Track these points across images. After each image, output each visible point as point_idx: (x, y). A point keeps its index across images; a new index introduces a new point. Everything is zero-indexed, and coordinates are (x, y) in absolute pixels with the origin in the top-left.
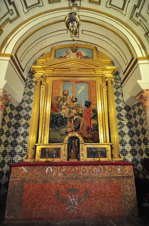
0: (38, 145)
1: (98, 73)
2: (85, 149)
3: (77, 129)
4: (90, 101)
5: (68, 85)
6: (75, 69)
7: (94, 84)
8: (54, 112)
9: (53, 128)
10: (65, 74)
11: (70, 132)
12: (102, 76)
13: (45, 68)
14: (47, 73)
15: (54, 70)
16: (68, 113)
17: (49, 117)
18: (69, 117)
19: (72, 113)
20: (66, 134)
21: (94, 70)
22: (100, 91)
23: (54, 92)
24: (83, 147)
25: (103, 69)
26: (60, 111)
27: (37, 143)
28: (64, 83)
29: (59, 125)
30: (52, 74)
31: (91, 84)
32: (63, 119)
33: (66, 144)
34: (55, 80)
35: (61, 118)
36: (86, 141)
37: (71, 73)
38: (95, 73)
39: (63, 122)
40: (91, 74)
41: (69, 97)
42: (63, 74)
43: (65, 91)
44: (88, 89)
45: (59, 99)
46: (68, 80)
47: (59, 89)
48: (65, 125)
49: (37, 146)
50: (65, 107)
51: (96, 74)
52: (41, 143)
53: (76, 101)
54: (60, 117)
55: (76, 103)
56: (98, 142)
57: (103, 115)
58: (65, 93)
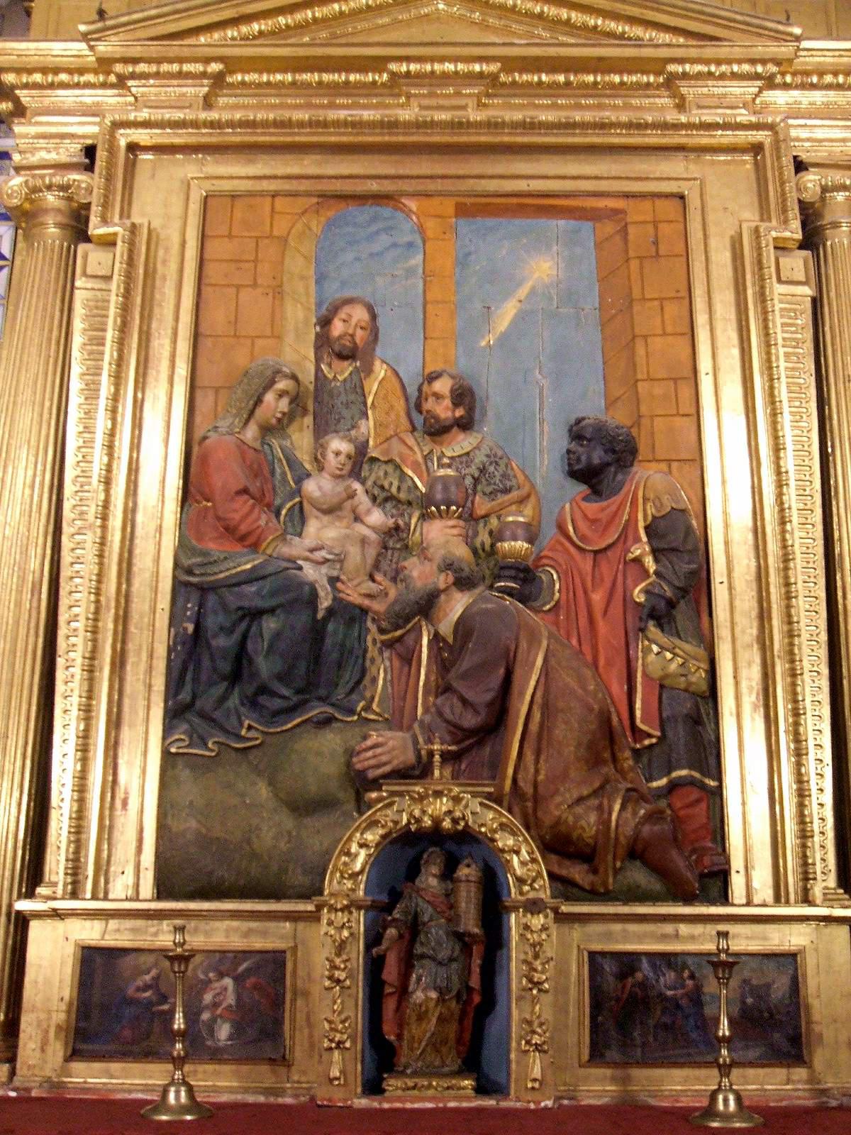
0: (39, 915)
1: (708, 117)
2: (562, 972)
3: (480, 743)
4: (619, 418)
5: (371, 237)
6: (449, 67)
7: (665, 229)
8: (215, 548)
10: (345, 124)
11: (402, 774)
12: (757, 149)
13: (119, 68)
14: (144, 115)
15: (218, 79)
16: (372, 552)
17: (164, 602)
18: (378, 606)
20: (347, 796)
21: (670, 83)
22: (732, 315)
23: (217, 317)
24: (549, 951)
25: (772, 68)
26: (282, 538)
27: (30, 894)
28: (330, 224)
29: (273, 694)
30: (195, 124)
31: (631, 230)
32: (317, 631)
34: (227, 186)
35: (301, 620)
37: (405, 115)
38: (681, 106)
39: (316, 658)
40: (630, 125)
41: (380, 371)
42: (325, 124)
43: (335, 309)
44: (601, 280)
45: (269, 397)
46: (374, 186)
47: (278, 292)
48: (340, 693)
49: (35, 927)
50: (340, 488)
51: (689, 126)
52: (74, 895)
53: (465, 425)
54: (288, 607)
55: (461, 444)
56: (715, 891)
57: (774, 580)
58: (338, 328)
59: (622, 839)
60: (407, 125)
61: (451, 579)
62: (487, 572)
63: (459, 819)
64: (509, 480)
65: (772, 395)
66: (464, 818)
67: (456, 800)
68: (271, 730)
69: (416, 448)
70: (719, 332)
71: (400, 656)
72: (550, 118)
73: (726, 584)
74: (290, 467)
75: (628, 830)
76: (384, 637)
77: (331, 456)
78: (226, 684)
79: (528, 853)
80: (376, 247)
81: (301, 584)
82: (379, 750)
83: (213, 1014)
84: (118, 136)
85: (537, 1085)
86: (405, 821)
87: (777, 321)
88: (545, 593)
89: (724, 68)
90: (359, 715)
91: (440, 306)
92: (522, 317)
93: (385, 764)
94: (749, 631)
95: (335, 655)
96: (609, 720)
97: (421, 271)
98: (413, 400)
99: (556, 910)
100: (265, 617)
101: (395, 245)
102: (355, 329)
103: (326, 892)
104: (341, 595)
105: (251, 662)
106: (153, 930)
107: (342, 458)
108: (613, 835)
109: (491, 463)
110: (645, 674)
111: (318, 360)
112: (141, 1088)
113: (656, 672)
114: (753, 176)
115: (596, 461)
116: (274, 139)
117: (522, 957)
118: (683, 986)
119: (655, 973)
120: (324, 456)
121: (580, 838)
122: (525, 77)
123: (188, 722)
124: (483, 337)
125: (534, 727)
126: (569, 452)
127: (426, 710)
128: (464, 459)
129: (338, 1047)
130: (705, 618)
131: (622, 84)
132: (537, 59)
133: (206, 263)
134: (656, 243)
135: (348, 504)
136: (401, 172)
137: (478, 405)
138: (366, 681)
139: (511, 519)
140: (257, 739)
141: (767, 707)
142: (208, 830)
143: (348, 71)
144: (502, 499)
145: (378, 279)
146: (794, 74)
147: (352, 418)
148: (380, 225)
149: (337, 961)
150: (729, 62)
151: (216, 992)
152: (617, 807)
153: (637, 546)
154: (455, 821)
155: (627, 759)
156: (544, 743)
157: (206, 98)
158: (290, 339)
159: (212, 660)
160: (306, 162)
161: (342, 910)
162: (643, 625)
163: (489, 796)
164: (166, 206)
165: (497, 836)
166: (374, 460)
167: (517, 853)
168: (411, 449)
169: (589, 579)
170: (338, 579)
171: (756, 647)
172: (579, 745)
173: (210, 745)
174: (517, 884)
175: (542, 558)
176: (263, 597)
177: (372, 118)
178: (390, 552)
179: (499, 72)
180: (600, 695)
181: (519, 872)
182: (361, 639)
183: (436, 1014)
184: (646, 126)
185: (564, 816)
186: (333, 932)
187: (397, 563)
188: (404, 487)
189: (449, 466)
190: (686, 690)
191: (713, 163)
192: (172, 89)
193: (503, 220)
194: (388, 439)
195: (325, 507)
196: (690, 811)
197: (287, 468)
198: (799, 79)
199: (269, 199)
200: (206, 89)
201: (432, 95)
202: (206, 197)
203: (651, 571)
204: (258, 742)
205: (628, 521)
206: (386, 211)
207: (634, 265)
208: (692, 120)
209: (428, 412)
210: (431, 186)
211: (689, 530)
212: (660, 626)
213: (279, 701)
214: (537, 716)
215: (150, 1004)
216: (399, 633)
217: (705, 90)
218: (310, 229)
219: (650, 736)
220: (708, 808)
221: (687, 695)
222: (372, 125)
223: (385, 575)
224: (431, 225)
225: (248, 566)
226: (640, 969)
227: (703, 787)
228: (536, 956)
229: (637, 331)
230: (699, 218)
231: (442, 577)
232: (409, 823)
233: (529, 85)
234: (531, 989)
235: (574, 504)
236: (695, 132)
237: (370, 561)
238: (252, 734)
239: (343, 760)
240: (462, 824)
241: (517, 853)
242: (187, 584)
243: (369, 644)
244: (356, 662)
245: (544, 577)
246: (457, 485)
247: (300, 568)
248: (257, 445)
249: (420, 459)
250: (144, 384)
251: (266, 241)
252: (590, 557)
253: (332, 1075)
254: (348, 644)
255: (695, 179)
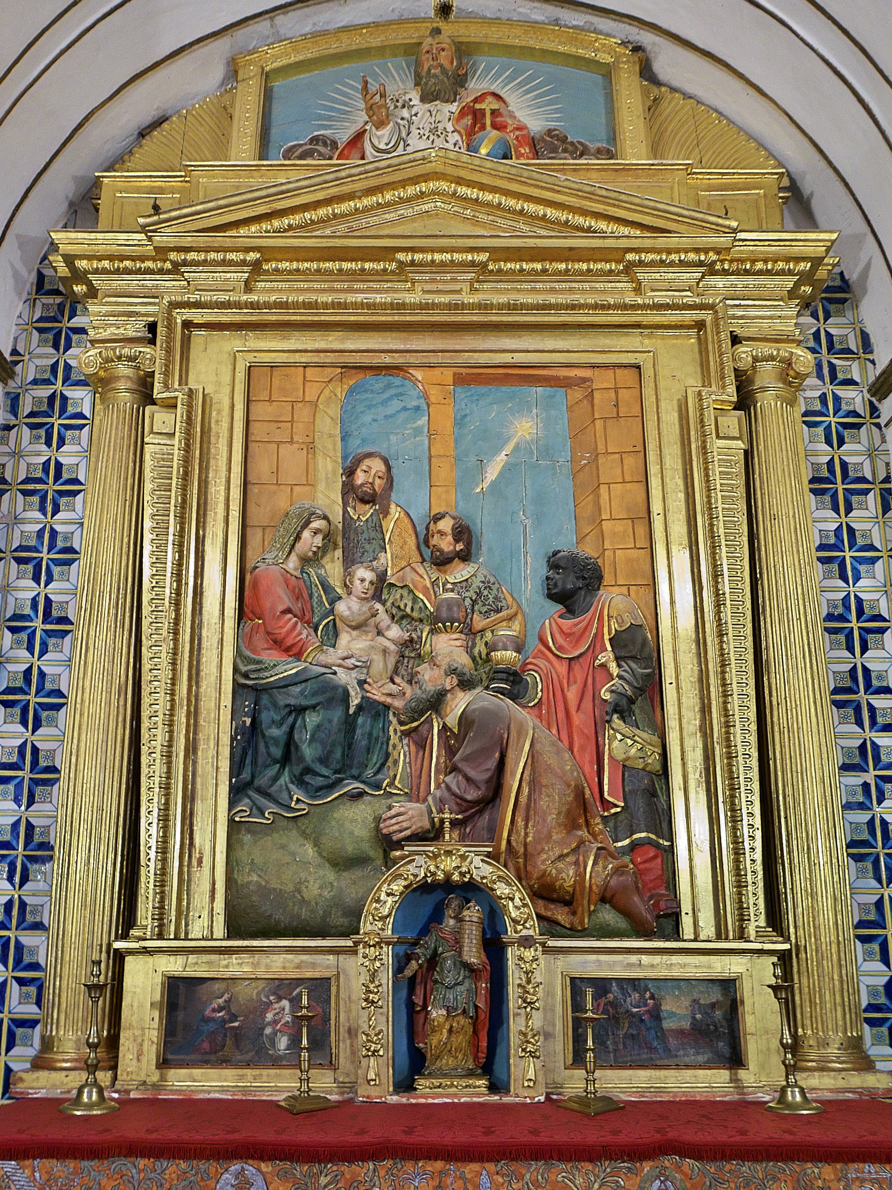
0: (132, 952)
2: (550, 993)
3: (480, 812)
4: (588, 550)
5: (385, 403)
9: (262, 801)
10: (362, 305)
11: (420, 837)
12: (700, 325)
13: (173, 256)
15: (256, 266)
16: (392, 661)
17: (227, 700)
18: (398, 703)
19: (433, 663)
20: (376, 854)
21: (629, 268)
23: (262, 468)
24: (538, 977)
25: (713, 256)
26: (320, 649)
27: (125, 936)
28: (351, 391)
30: (238, 305)
31: (597, 395)
32: (349, 723)
33: (378, 945)
35: (337, 715)
36: (561, 915)
38: (638, 290)
39: (350, 745)
40: (596, 306)
41: (395, 512)
42: (344, 306)
43: (358, 461)
45: (306, 534)
46: (387, 359)
47: (311, 447)
48: (369, 772)
49: (128, 959)
52: (160, 936)
53: (465, 557)
54: (328, 704)
55: (460, 572)
58: (360, 478)
59: (594, 887)
60: (413, 306)
61: (455, 681)
62: (484, 676)
63: (465, 872)
64: (501, 601)
65: (712, 531)
66: (469, 872)
67: (463, 857)
68: (315, 803)
69: (425, 577)
70: (667, 480)
71: (416, 743)
72: (530, 301)
73: (674, 684)
74: (325, 592)
75: (599, 881)
76: (403, 728)
77: (357, 583)
78: (278, 765)
79: (521, 900)
80: (390, 411)
81: (335, 688)
82: (401, 818)
83: (274, 1029)
84: (174, 314)
85: (531, 1084)
86: (423, 875)
87: (716, 470)
88: (530, 691)
89: (674, 257)
90: (385, 789)
91: (443, 459)
92: (509, 469)
93: (406, 829)
94: (693, 722)
95: (364, 743)
96: (583, 794)
97: (426, 430)
98: (422, 537)
99: (543, 945)
100: (307, 712)
101: (405, 409)
102: (374, 479)
103: (362, 932)
104: (368, 695)
105: (297, 747)
106: (225, 962)
107: (367, 583)
108: (587, 885)
109: (486, 588)
110: (610, 756)
111: (345, 504)
112: (217, 1088)
113: (620, 756)
114: (696, 349)
115: (570, 586)
116: (303, 318)
117: (519, 981)
118: (646, 1005)
119: (623, 994)
120: (351, 582)
121: (561, 886)
122: (509, 265)
123: (249, 797)
124: (477, 485)
125: (523, 799)
126: (548, 578)
127: (438, 786)
128: (464, 584)
129: (373, 1055)
130: (658, 710)
131: (589, 270)
132: (519, 249)
133: (251, 423)
134: (616, 406)
135: (372, 621)
136: (408, 347)
137: (474, 540)
138: (390, 763)
139: (502, 633)
140: (304, 809)
141: (708, 782)
142: (267, 882)
143: (363, 260)
144: (494, 617)
145: (392, 437)
146: (731, 261)
147: (374, 552)
148: (393, 392)
149: (372, 986)
150: (678, 251)
151: (276, 1011)
152: (590, 863)
153: (603, 654)
154: (463, 874)
155: (598, 824)
156: (532, 813)
157: (247, 282)
158: (321, 486)
159: (267, 747)
160: (330, 339)
161: (374, 946)
162: (608, 718)
163: (489, 855)
164: (217, 375)
165: (495, 886)
166: (392, 585)
167: (512, 899)
168: (422, 577)
169: (565, 681)
170: (365, 682)
171: (699, 734)
172: (559, 814)
173: (266, 815)
174: (512, 924)
175: (528, 664)
176: (306, 696)
177: (383, 300)
178: (406, 660)
179: (488, 261)
180: (575, 774)
181: (513, 915)
182: (385, 730)
183: (447, 1027)
184: (609, 307)
185: (549, 869)
186: (367, 963)
187: (412, 668)
188: (417, 607)
189: (452, 591)
190: (643, 769)
191: (663, 337)
192: (217, 274)
193: (493, 388)
194: (402, 569)
195: (353, 624)
196: (647, 865)
197: (322, 592)
198: (734, 266)
199: (301, 369)
200: (247, 274)
201: (433, 281)
202: (250, 367)
203: (615, 674)
204: (304, 812)
205: (596, 635)
206: (397, 381)
207: (599, 424)
208: (647, 301)
209: (434, 546)
210: (433, 359)
211: (645, 641)
212: (623, 718)
213: (321, 779)
214: (526, 790)
215: (224, 1021)
216: (415, 724)
217: (657, 276)
218: (336, 395)
219: (616, 806)
220: (662, 861)
221: (644, 773)
222: (383, 306)
223: (403, 678)
224: (434, 394)
225: (294, 671)
226: (610, 992)
227: (658, 846)
228: (529, 982)
229: (602, 480)
230: (652, 385)
231: (448, 680)
232: (426, 876)
233: (513, 272)
234: (525, 1008)
235: (552, 621)
236: (649, 312)
237: (391, 666)
238: (302, 806)
239: (373, 825)
240: (468, 876)
241: (512, 899)
242: (244, 686)
243: (392, 733)
244: (381, 748)
245: (529, 679)
246: (459, 606)
247: (335, 673)
248: (297, 573)
249: (429, 585)
250: (204, 523)
251: (300, 405)
252: (565, 664)
253: (369, 1078)
254: (375, 734)
255: (649, 352)
